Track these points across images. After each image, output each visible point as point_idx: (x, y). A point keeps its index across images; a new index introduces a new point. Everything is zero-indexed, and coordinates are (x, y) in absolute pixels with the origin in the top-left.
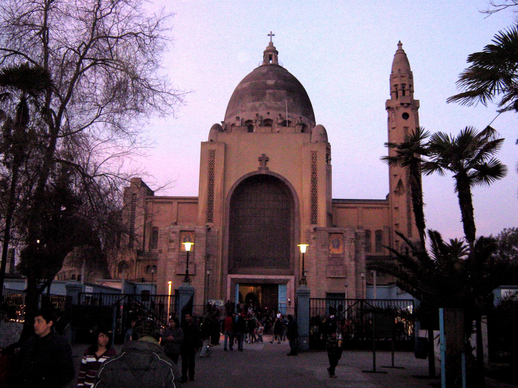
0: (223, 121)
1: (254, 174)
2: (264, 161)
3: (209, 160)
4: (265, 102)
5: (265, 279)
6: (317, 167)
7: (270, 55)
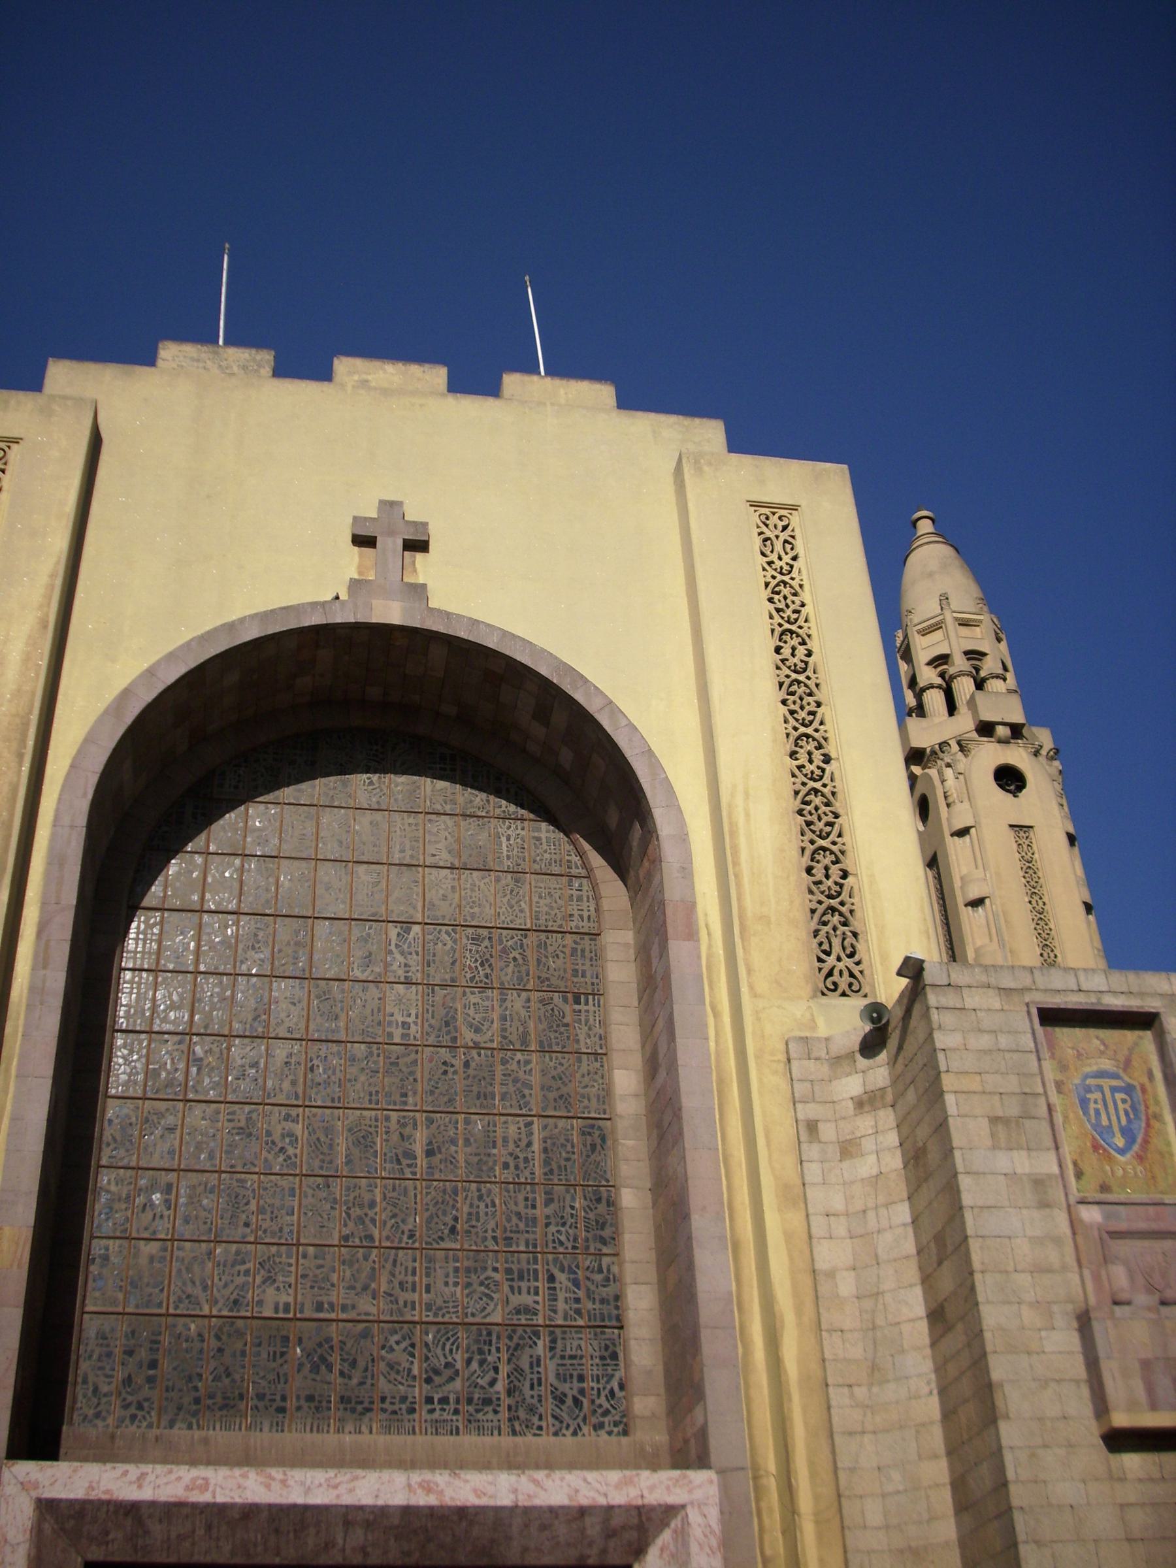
2: (391, 545)
5: (407, 1511)
6: (806, 596)
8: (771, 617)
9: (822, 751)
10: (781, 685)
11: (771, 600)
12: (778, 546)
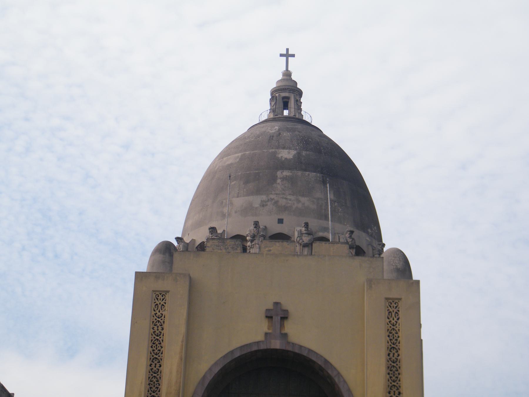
0: (180, 236)
1: (255, 348)
2: (277, 319)
3: (153, 313)
4: (272, 196)
6: (400, 334)
7: (284, 98)
8: (388, 343)
9: (398, 391)
10: (388, 367)
11: (389, 336)
12: (393, 314)
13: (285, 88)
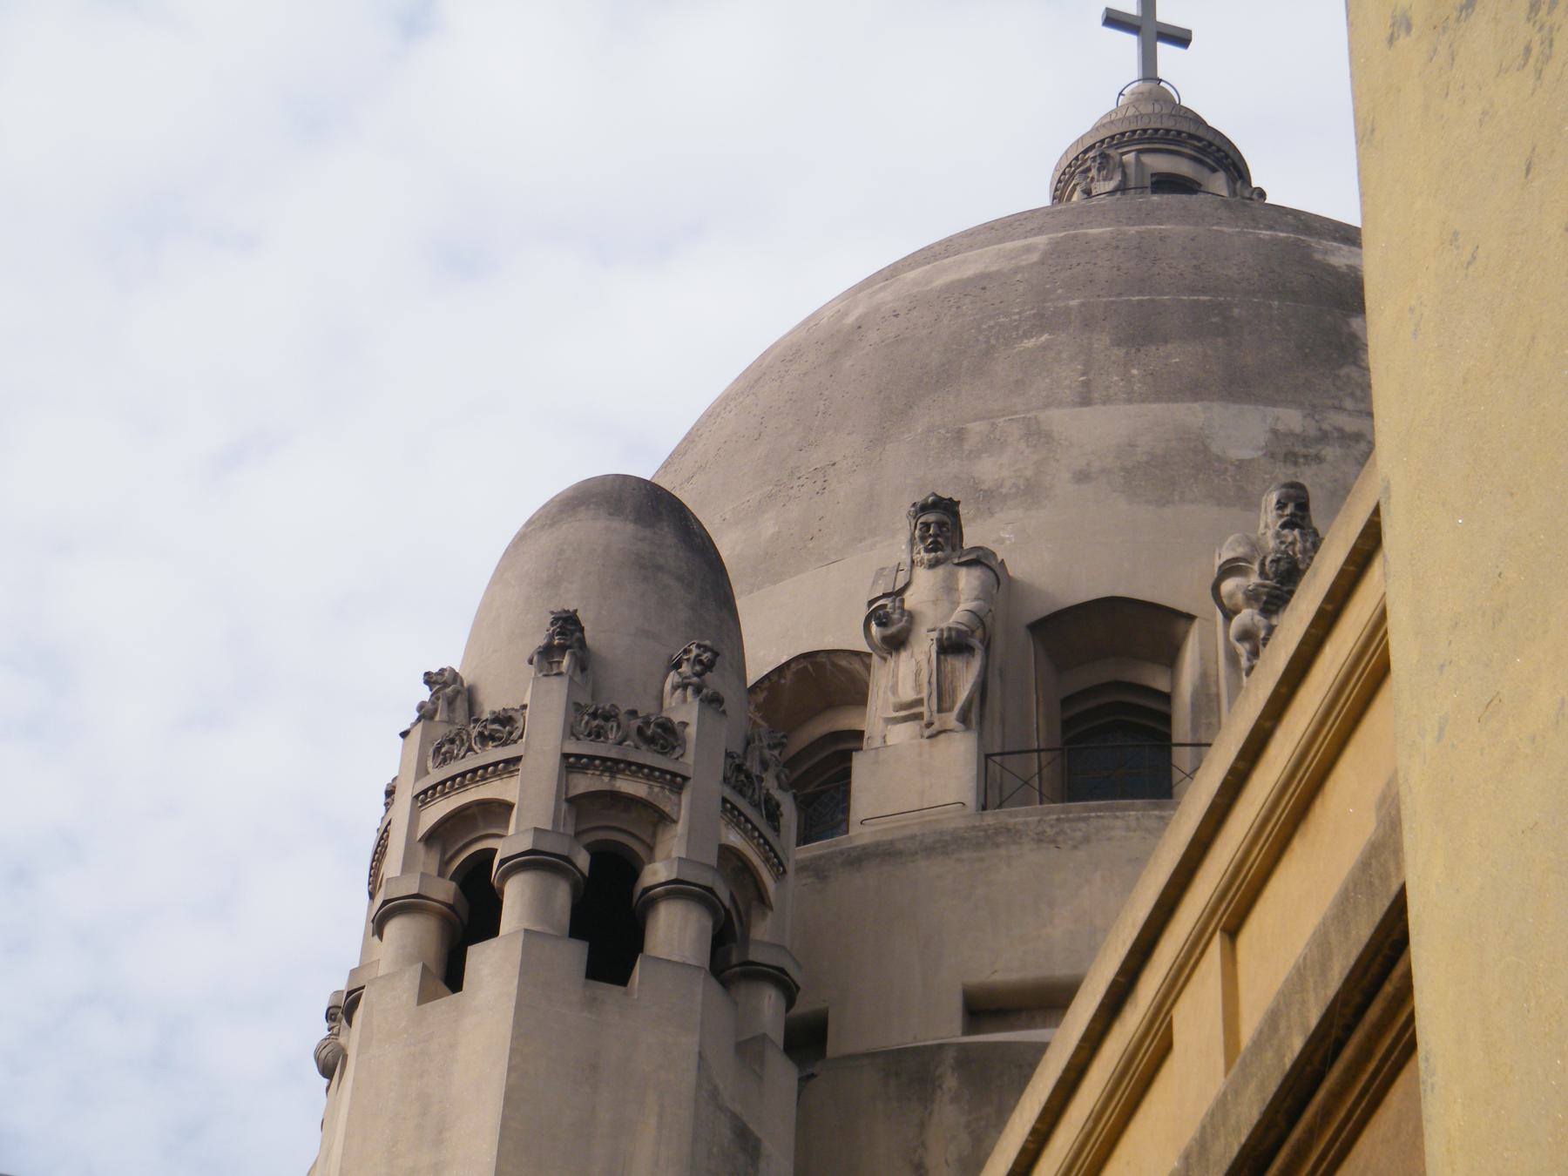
13: (1178, 127)
